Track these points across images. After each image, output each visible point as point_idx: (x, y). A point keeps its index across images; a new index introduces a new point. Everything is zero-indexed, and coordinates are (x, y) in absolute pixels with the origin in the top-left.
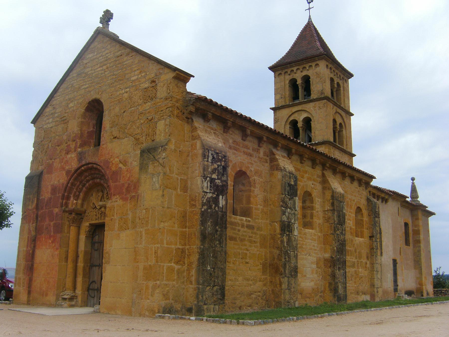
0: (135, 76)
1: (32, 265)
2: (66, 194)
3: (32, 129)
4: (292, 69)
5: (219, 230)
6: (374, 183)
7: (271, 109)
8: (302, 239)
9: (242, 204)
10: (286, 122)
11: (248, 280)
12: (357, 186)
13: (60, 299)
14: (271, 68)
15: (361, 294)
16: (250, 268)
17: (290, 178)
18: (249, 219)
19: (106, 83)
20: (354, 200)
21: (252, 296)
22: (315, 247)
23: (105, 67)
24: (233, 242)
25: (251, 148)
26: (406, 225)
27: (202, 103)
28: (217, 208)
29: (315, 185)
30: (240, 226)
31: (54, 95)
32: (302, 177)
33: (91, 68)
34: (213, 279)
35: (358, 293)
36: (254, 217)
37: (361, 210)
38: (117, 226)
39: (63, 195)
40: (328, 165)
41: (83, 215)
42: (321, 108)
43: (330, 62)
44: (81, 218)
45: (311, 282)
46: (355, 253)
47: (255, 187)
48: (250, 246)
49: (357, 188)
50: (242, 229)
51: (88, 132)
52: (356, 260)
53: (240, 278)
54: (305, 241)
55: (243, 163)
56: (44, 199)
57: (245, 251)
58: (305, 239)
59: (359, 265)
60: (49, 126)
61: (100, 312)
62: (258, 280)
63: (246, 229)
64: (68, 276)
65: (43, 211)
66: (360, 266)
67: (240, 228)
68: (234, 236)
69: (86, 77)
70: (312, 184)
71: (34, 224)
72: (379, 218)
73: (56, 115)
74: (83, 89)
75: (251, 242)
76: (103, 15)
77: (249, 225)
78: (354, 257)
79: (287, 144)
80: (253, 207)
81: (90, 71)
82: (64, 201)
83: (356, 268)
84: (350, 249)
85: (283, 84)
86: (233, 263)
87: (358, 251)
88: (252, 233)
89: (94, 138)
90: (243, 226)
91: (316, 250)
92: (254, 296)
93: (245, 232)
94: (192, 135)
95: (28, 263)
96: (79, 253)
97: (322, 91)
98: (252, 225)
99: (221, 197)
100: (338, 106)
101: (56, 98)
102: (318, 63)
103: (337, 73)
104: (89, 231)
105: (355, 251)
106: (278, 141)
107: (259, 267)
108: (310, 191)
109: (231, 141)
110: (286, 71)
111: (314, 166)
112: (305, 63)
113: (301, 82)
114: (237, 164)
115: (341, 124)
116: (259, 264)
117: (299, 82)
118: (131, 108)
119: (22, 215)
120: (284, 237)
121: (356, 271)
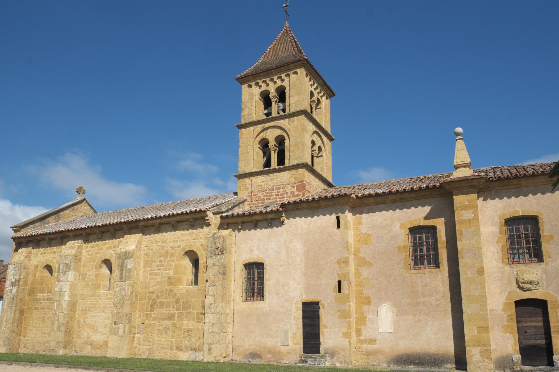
8: (95, 300)
11: (44, 333)
15: (184, 350)
16: (46, 326)
30: (43, 300)
35: (179, 348)
46: (175, 304)
48: (48, 312)
52: (177, 312)
53: (39, 333)
54: (98, 302)
55: (49, 259)
57: (44, 316)
58: (99, 300)
59: (184, 317)
63: (46, 301)
68: (38, 306)
70: (113, 251)
84: (167, 300)
87: (181, 301)
88: (50, 303)
93: (45, 303)
99: (14, 287)
105: (177, 301)
121: (174, 325)
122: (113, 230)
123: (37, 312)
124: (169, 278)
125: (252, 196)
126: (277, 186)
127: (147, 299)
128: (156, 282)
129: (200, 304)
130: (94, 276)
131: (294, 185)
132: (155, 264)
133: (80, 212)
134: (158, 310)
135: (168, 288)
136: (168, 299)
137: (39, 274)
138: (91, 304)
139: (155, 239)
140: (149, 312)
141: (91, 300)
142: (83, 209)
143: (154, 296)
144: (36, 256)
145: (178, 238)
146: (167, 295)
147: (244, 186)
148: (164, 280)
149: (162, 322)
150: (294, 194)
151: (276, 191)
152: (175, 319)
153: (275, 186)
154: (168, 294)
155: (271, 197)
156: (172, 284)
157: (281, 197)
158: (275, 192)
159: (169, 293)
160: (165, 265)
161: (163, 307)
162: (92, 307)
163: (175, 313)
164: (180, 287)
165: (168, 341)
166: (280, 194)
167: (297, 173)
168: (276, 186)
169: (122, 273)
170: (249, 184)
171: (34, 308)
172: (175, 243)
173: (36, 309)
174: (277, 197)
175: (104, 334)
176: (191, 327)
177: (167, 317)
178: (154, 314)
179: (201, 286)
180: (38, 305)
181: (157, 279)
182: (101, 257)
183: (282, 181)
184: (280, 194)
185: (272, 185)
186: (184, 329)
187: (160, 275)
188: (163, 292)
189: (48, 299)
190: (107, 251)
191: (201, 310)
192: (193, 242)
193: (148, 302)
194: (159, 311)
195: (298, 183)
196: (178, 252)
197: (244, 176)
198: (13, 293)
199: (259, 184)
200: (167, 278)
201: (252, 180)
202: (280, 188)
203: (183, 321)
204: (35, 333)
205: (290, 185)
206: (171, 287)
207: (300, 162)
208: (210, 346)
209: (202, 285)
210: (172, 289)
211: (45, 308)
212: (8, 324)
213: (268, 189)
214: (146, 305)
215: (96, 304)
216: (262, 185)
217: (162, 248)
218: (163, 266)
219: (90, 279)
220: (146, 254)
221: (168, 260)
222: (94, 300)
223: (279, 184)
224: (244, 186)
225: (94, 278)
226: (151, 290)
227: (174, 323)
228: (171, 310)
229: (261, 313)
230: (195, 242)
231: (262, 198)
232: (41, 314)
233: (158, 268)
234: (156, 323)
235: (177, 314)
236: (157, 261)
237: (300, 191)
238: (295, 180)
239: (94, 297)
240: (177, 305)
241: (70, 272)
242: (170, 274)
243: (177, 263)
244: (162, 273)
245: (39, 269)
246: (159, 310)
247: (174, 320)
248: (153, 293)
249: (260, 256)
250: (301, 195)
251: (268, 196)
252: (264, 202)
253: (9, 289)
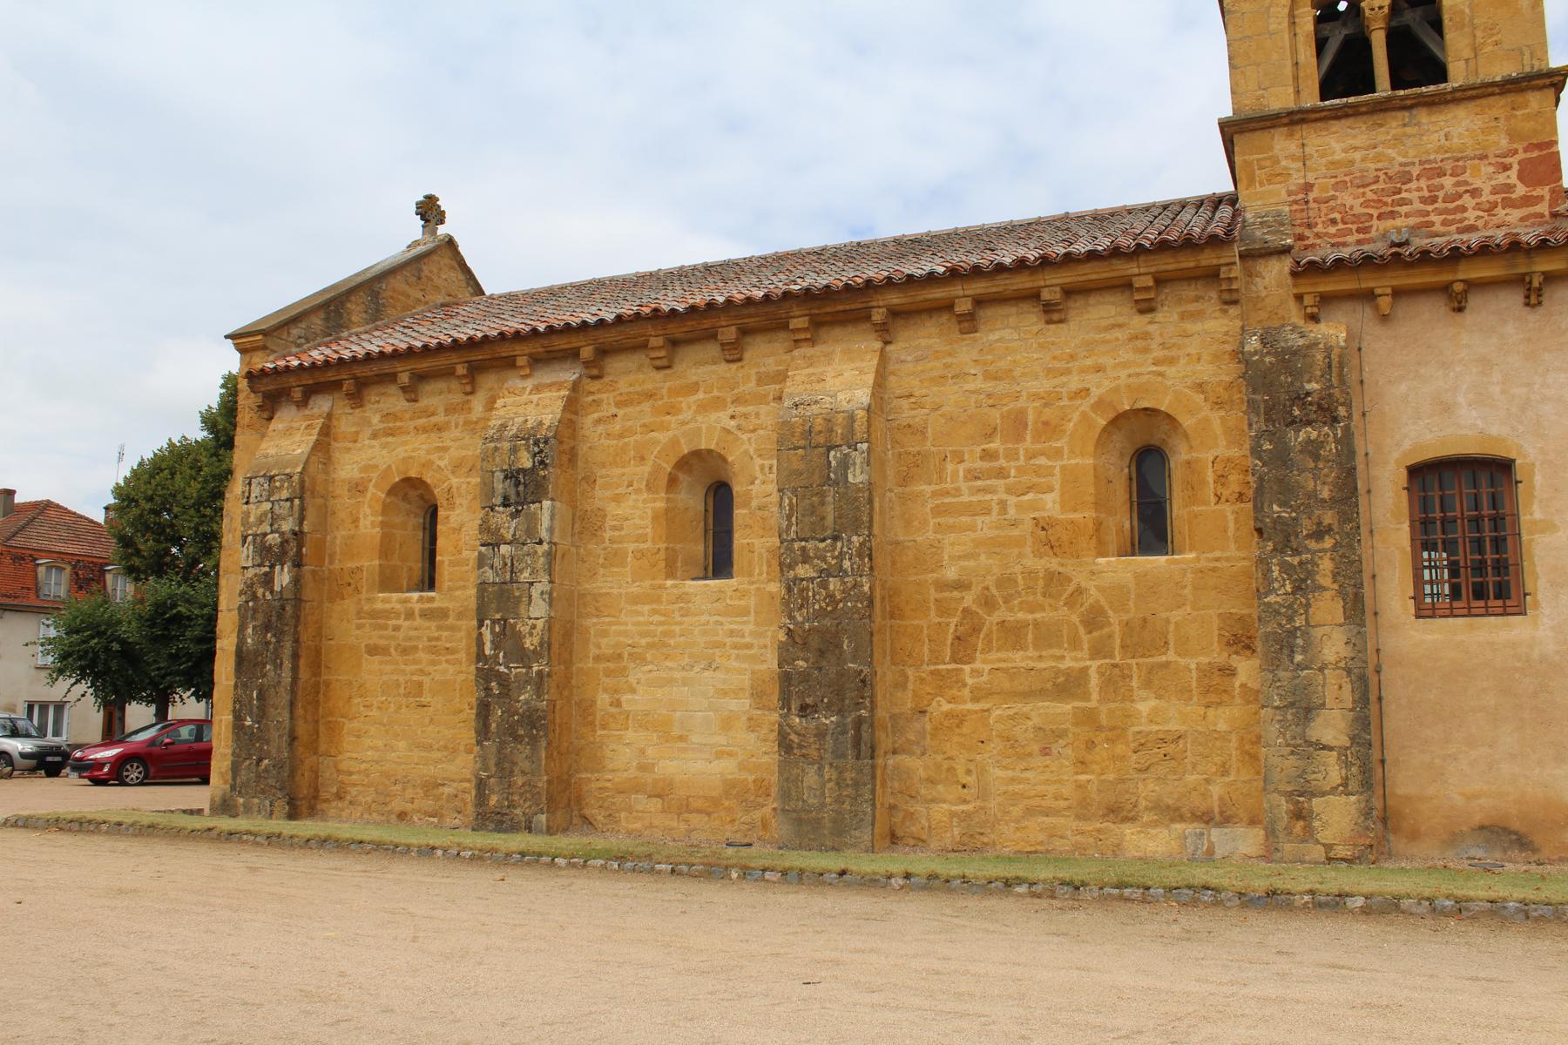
5: (273, 640)
8: (663, 619)
11: (429, 748)
17: (514, 450)
20: (1084, 392)
21: (441, 789)
22: (743, 636)
24: (377, 658)
28: (269, 597)
29: (745, 416)
30: (403, 616)
32: (669, 414)
34: (258, 745)
35: (1118, 812)
36: (446, 584)
45: (718, 758)
46: (1082, 630)
47: (452, 506)
48: (433, 663)
50: (407, 623)
52: (1094, 664)
53: (402, 744)
54: (680, 623)
57: (415, 678)
58: (682, 616)
62: (462, 748)
63: (418, 621)
67: (400, 622)
68: (383, 642)
70: (733, 417)
75: (433, 650)
76: (439, 207)
80: (443, 562)
83: (1095, 696)
84: (1038, 616)
86: (379, 708)
87: (1114, 618)
88: (439, 628)
90: (410, 615)
91: (749, 646)
92: (447, 790)
93: (416, 629)
99: (278, 568)
105: (1094, 620)
107: (463, 716)
109: (376, 419)
114: (394, 468)
116: (466, 706)
120: (484, 628)
122: (733, 329)
123: (381, 663)
124: (1043, 525)
125: (1312, 205)
126: (1427, 166)
127: (933, 613)
128: (973, 541)
129: (1216, 632)
130: (643, 519)
131: (1507, 160)
132: (961, 468)
133: (437, 289)
134: (994, 655)
135: (1042, 564)
136: (1044, 610)
137: (372, 515)
138: (642, 634)
139: (947, 366)
140: (949, 667)
141: (641, 619)
142: (446, 280)
143: (969, 599)
144: (351, 445)
145: (1072, 357)
146: (1035, 594)
147: (1263, 163)
148: (1016, 532)
149: (1019, 707)
150: (1513, 196)
151: (1423, 183)
152: (1090, 695)
153: (1414, 164)
154: (1039, 590)
155: (1404, 209)
156: (1057, 550)
157: (1451, 206)
158: (1419, 189)
159: (1046, 586)
160: (1013, 472)
161: (1018, 645)
162: (650, 646)
163: (1084, 671)
164: (1101, 560)
165: (1059, 782)
166: (1441, 194)
167: (1518, 113)
168: (1421, 163)
170: (1293, 158)
171: (363, 649)
172: (1057, 381)
173: (373, 650)
174: (1430, 208)
175: (720, 755)
176: (1173, 726)
177: (1049, 685)
178: (976, 673)
179: (1210, 555)
180: (381, 637)
181: (974, 532)
182: (674, 442)
183: (1447, 144)
184: (1441, 194)
185: (1403, 160)
186: (1139, 733)
187: (988, 512)
188: (1016, 582)
189: (425, 614)
190: (700, 418)
191: (1219, 654)
192: (1149, 373)
193: (940, 623)
194: (1000, 660)
195: (1525, 151)
196: (1076, 416)
197: (1268, 124)
198: (277, 588)
199: (1336, 157)
200: (1028, 525)
201: (1305, 142)
202: (1442, 174)
203: (1133, 701)
204: (380, 743)
205: (1486, 162)
206: (1054, 564)
207: (1527, 69)
208: (1299, 802)
209: (1217, 554)
210: (1061, 569)
211: (415, 648)
213: (1382, 177)
214: (929, 636)
215: (665, 634)
216: (1352, 162)
217: (991, 402)
218: (1001, 473)
219: (623, 533)
220: (909, 426)
221: (1027, 450)
222: (656, 618)
223: (1432, 157)
224: (1263, 163)
225: (648, 530)
226: (951, 573)
227: (1084, 709)
228: (1063, 657)
229: (1518, 665)
230: (1160, 374)
231: (1358, 210)
232: (403, 672)
233: (979, 483)
234: (988, 710)
235: (1101, 674)
236: (966, 457)
237: (1541, 183)
238: (1511, 141)
239: (655, 606)
240: (1096, 634)
241: (546, 504)
242: (1044, 510)
243: (1078, 464)
244: (1003, 505)
245: (369, 495)
246: (1001, 655)
247: (1088, 699)
248: (960, 585)
249: (1494, 430)
250: (1547, 197)
251: (1386, 204)
252: (1371, 226)
253: (256, 575)
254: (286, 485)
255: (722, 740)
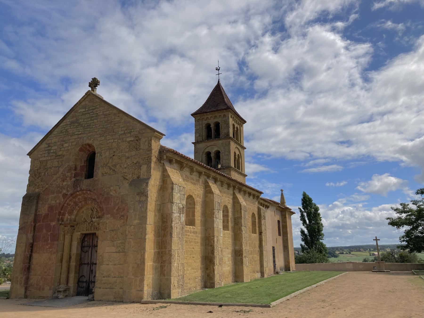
0: (122, 131)
1: (29, 266)
2: (62, 211)
3: (28, 160)
4: (208, 116)
6: (262, 196)
7: (192, 143)
9: (190, 217)
10: (203, 153)
12: (252, 199)
13: (56, 292)
14: (192, 115)
18: (194, 227)
19: (97, 133)
23: (95, 121)
25: (195, 180)
26: (279, 222)
27: (171, 153)
31: (49, 135)
33: (83, 120)
37: (254, 214)
38: (109, 236)
39: (60, 212)
40: (237, 187)
41: (75, 227)
42: (227, 144)
43: (233, 114)
44: (74, 229)
45: (228, 267)
49: (252, 200)
50: (191, 234)
51: (81, 166)
52: (253, 249)
53: (190, 268)
56: (42, 215)
60: (45, 159)
61: (94, 300)
63: (192, 234)
64: (62, 273)
65: (40, 223)
66: (255, 253)
67: (189, 234)
69: (79, 126)
71: (31, 234)
72: (265, 219)
73: (52, 151)
74: (77, 134)
77: (194, 231)
78: (251, 247)
79: (216, 175)
81: (82, 122)
82: (61, 217)
85: (201, 126)
87: (253, 243)
88: (196, 236)
89: (85, 170)
94: (164, 174)
95: (26, 265)
96: (72, 255)
97: (228, 133)
98: (196, 231)
100: (237, 143)
101: (51, 138)
102: (225, 114)
103: (237, 121)
104: (80, 239)
106: (210, 174)
108: (226, 205)
110: (203, 117)
111: (229, 188)
112: (216, 113)
113: (214, 126)
114: (188, 191)
115: (238, 155)
117: (212, 126)
118: (119, 153)
119: (19, 227)
169: (245, 221)
176: (257, 259)
212: (180, 259)
254: (183, 190)
255: (228, 263)
